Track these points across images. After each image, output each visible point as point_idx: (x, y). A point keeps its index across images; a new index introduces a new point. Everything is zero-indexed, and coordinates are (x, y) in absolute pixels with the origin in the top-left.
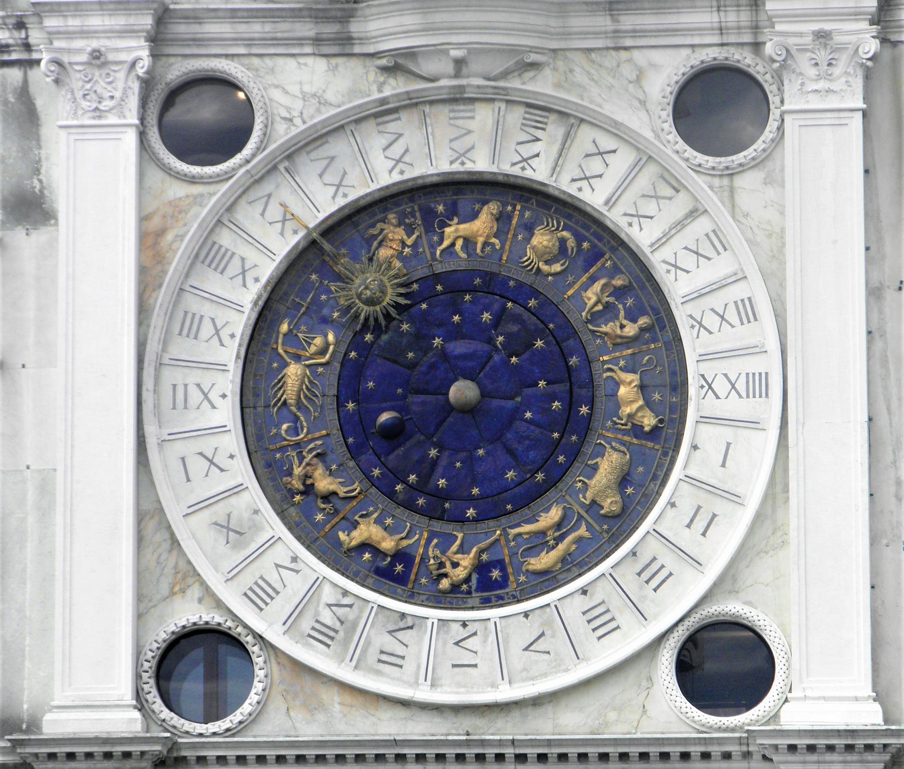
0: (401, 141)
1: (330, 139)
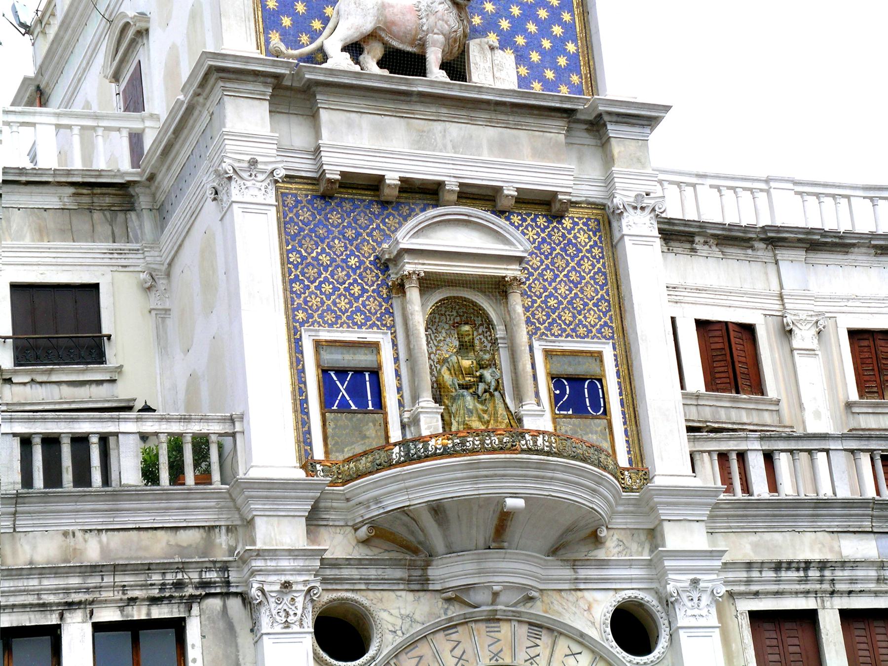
0: (460, 645)
1: (419, 644)
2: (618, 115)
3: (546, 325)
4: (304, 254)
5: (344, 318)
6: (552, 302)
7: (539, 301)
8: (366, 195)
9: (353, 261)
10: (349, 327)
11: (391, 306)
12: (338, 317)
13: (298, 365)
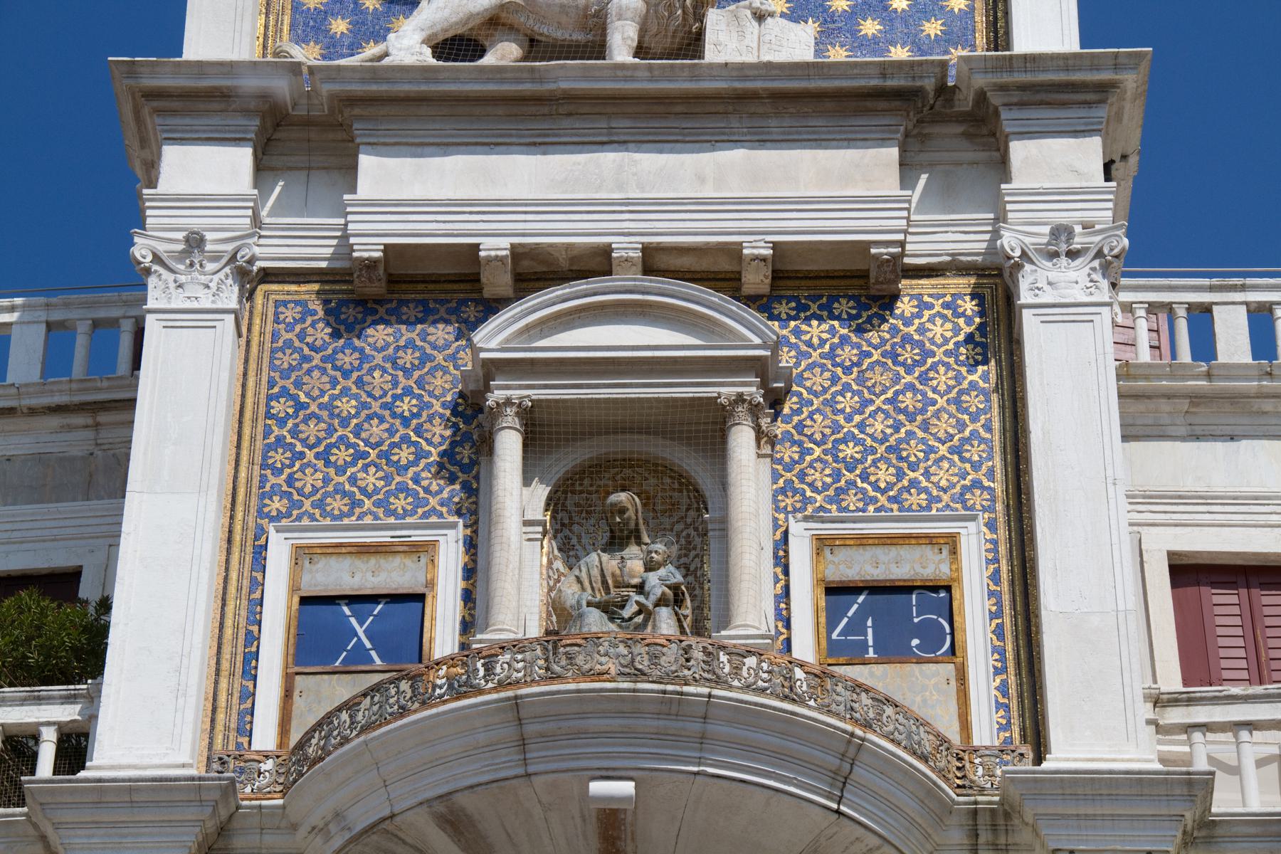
2: (1023, 87)
3: (831, 492)
4: (303, 398)
6: (849, 451)
8: (454, 291)
10: (376, 518)
11: (477, 478)
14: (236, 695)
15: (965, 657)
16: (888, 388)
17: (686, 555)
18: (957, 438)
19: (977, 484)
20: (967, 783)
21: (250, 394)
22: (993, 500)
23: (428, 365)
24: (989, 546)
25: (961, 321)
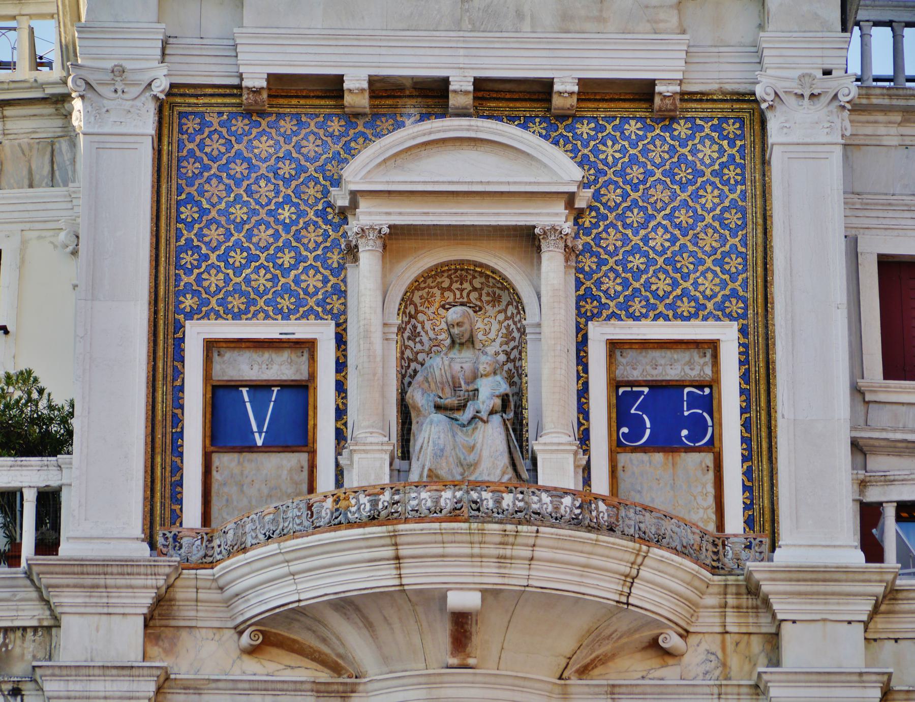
5: (261, 303)
6: (637, 261)
7: (611, 261)
8: (321, 107)
9: (286, 214)
11: (344, 281)
12: (251, 302)
13: (174, 380)
14: (168, 469)
15: (721, 448)
16: (667, 205)
17: (507, 343)
18: (719, 251)
19: (734, 292)
20: (720, 565)
21: (163, 200)
22: (746, 308)
23: (303, 176)
24: (742, 349)
25: (725, 143)
